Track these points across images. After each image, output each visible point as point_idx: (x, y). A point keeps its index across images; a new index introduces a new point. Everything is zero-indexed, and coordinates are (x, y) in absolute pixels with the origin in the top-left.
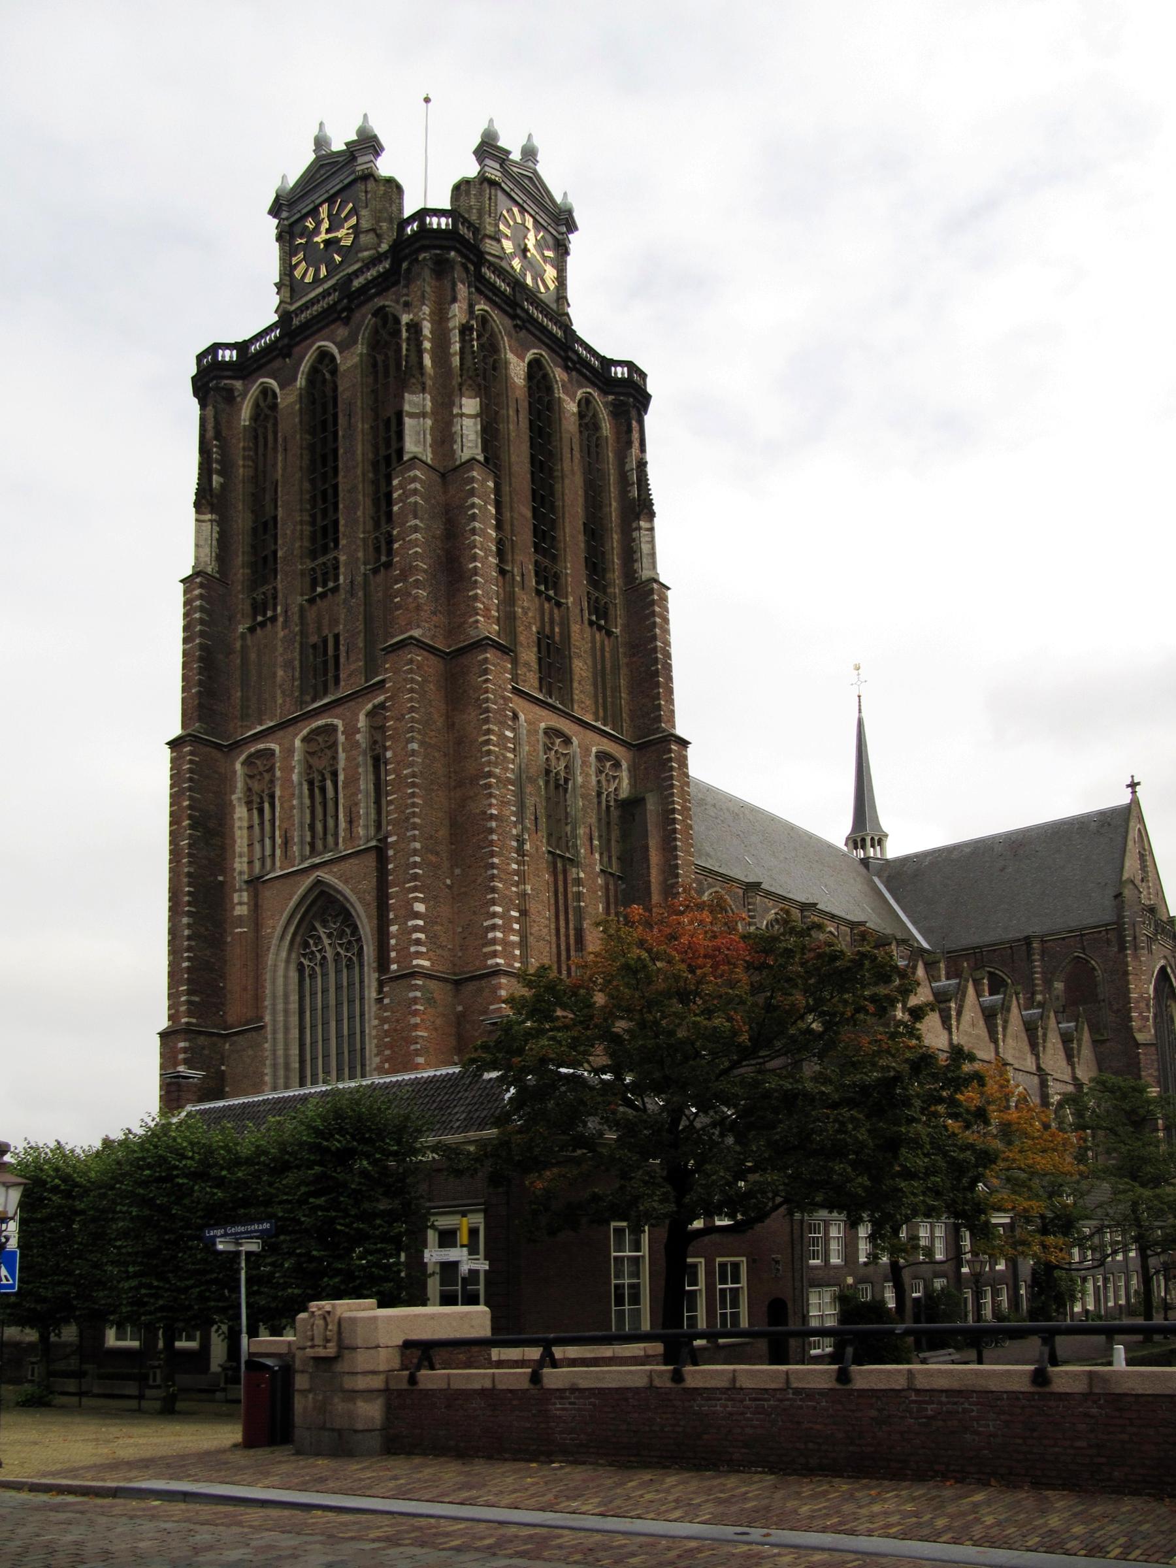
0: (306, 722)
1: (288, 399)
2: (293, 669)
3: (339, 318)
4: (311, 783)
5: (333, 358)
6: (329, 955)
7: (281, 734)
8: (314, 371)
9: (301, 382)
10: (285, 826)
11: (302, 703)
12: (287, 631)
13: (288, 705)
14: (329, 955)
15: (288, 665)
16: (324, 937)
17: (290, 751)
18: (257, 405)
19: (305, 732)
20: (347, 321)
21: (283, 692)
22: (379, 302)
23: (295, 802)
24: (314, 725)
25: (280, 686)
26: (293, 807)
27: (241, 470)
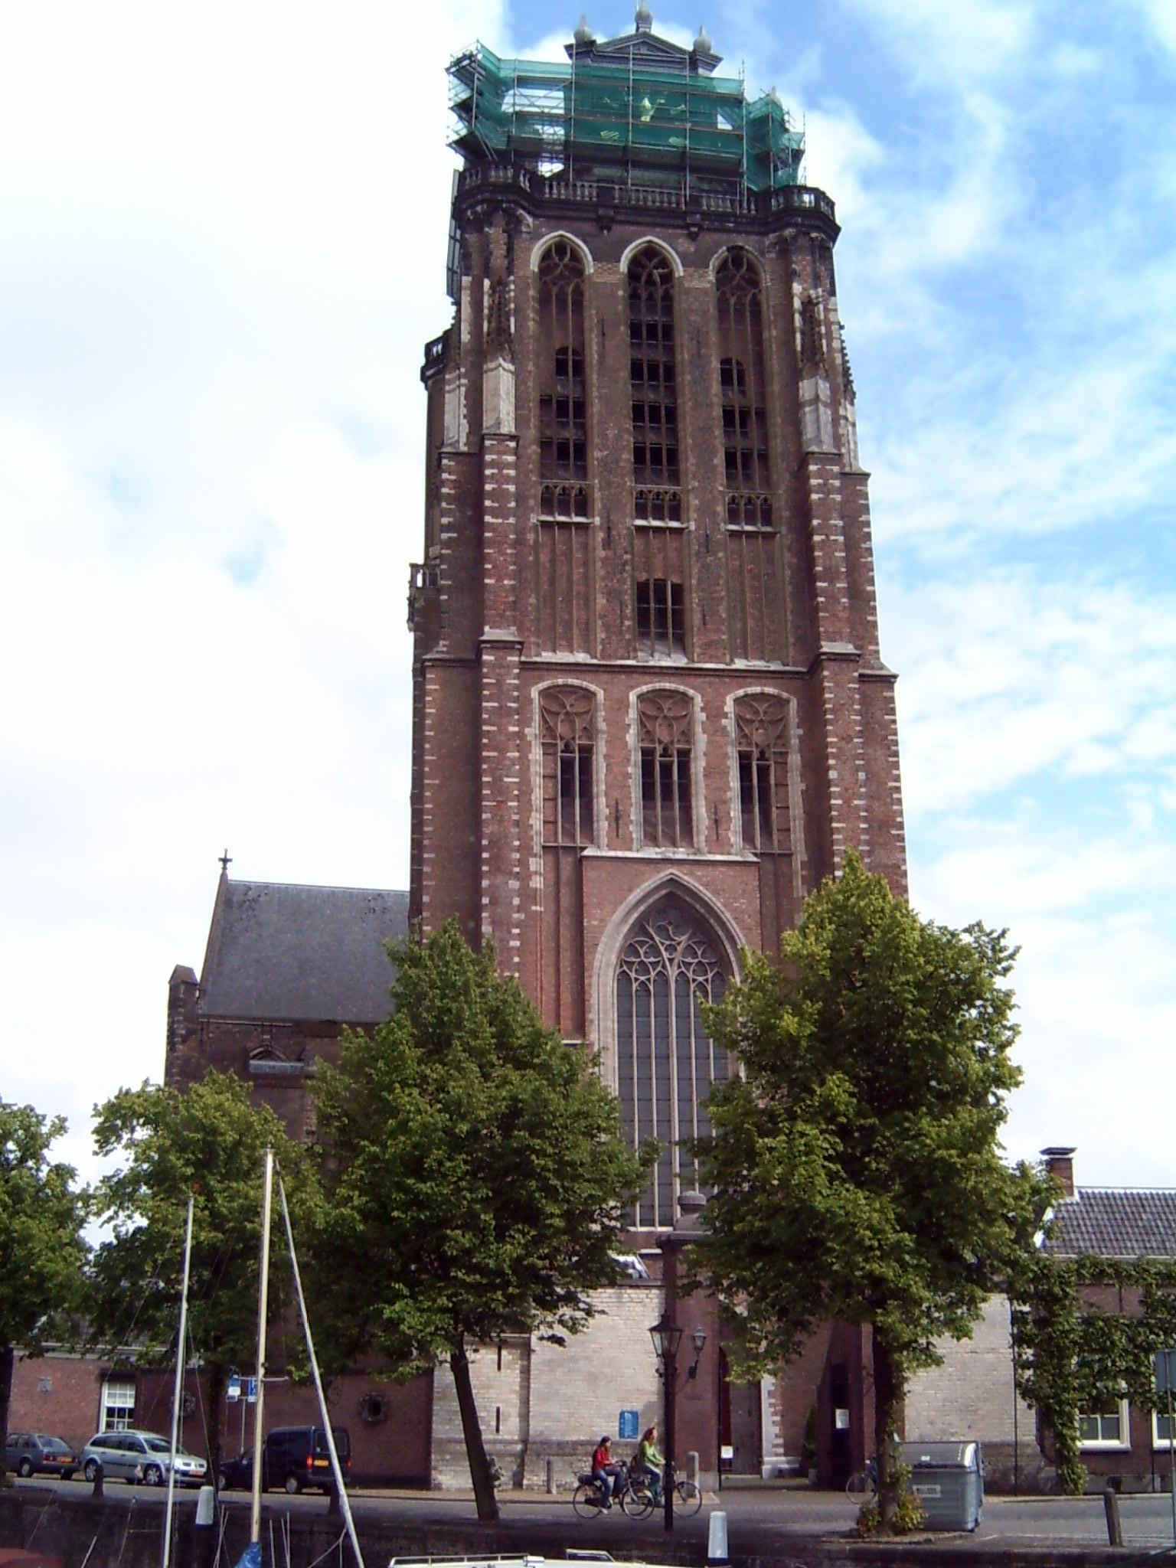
0: (647, 678)
1: (606, 275)
2: (622, 604)
3: (687, 226)
4: (647, 753)
5: (665, 263)
6: (672, 973)
7: (606, 677)
8: (634, 262)
9: (623, 266)
10: (616, 794)
11: (630, 651)
12: (610, 553)
13: (614, 645)
14: (672, 973)
15: (612, 594)
16: (662, 949)
17: (623, 705)
18: (546, 256)
19: (645, 688)
20: (693, 237)
21: (607, 627)
22: (748, 243)
23: (630, 770)
24: (658, 686)
25: (603, 617)
26: (628, 776)
27: (531, 324)
